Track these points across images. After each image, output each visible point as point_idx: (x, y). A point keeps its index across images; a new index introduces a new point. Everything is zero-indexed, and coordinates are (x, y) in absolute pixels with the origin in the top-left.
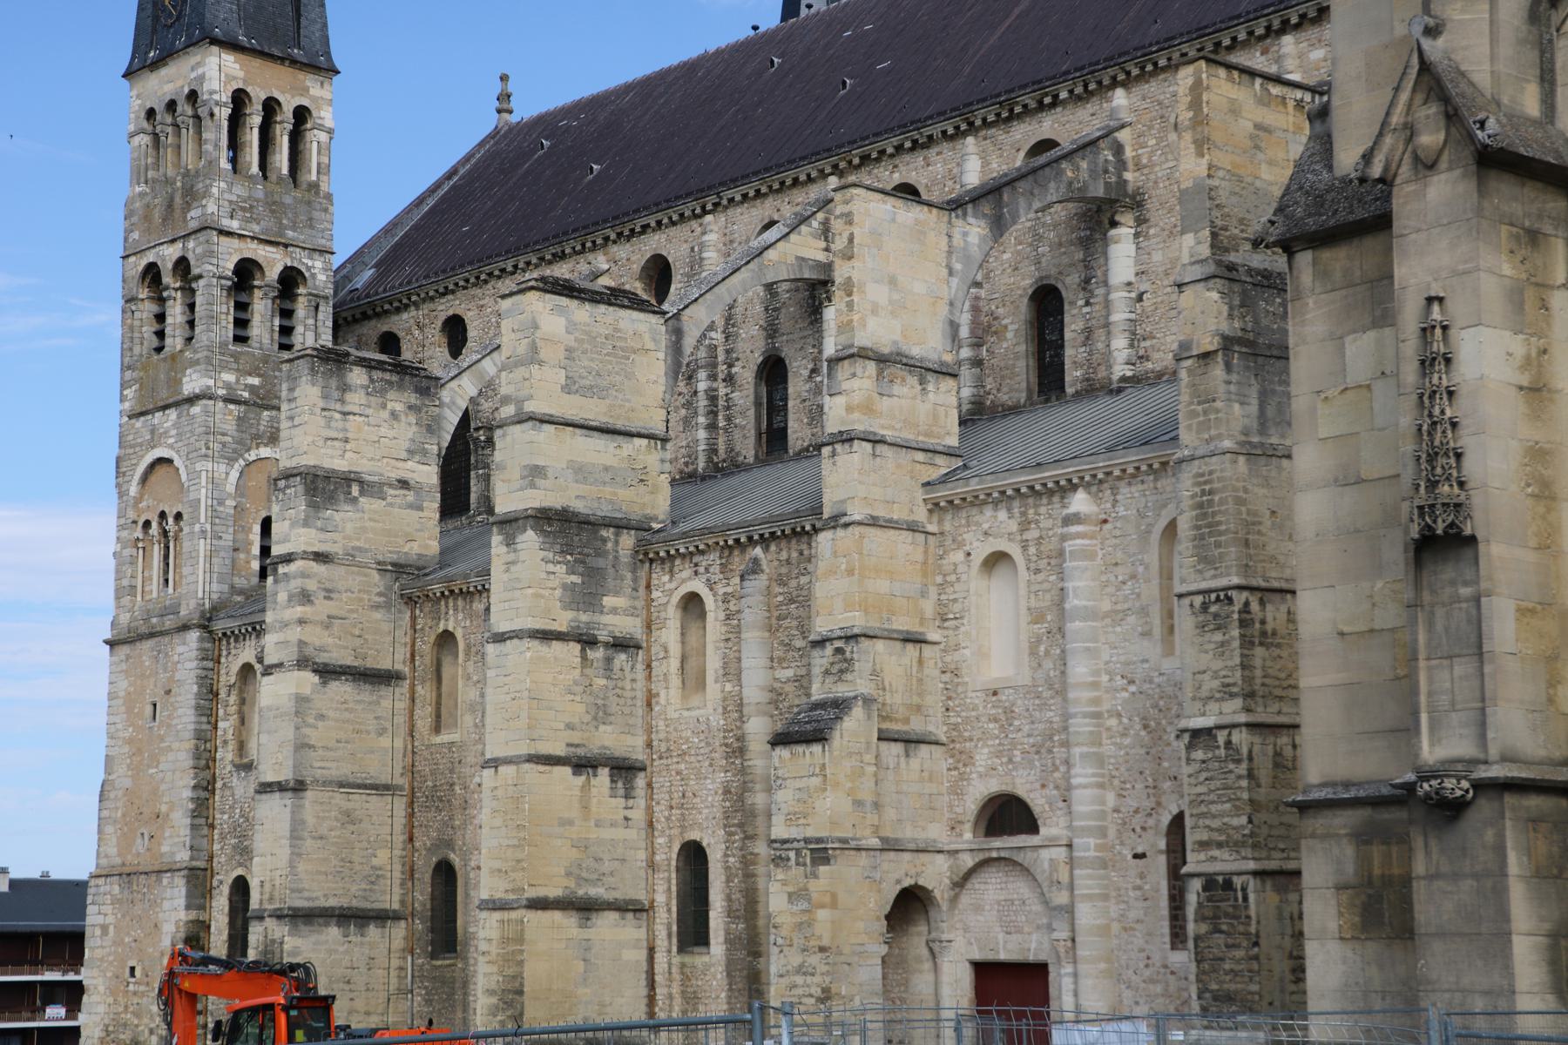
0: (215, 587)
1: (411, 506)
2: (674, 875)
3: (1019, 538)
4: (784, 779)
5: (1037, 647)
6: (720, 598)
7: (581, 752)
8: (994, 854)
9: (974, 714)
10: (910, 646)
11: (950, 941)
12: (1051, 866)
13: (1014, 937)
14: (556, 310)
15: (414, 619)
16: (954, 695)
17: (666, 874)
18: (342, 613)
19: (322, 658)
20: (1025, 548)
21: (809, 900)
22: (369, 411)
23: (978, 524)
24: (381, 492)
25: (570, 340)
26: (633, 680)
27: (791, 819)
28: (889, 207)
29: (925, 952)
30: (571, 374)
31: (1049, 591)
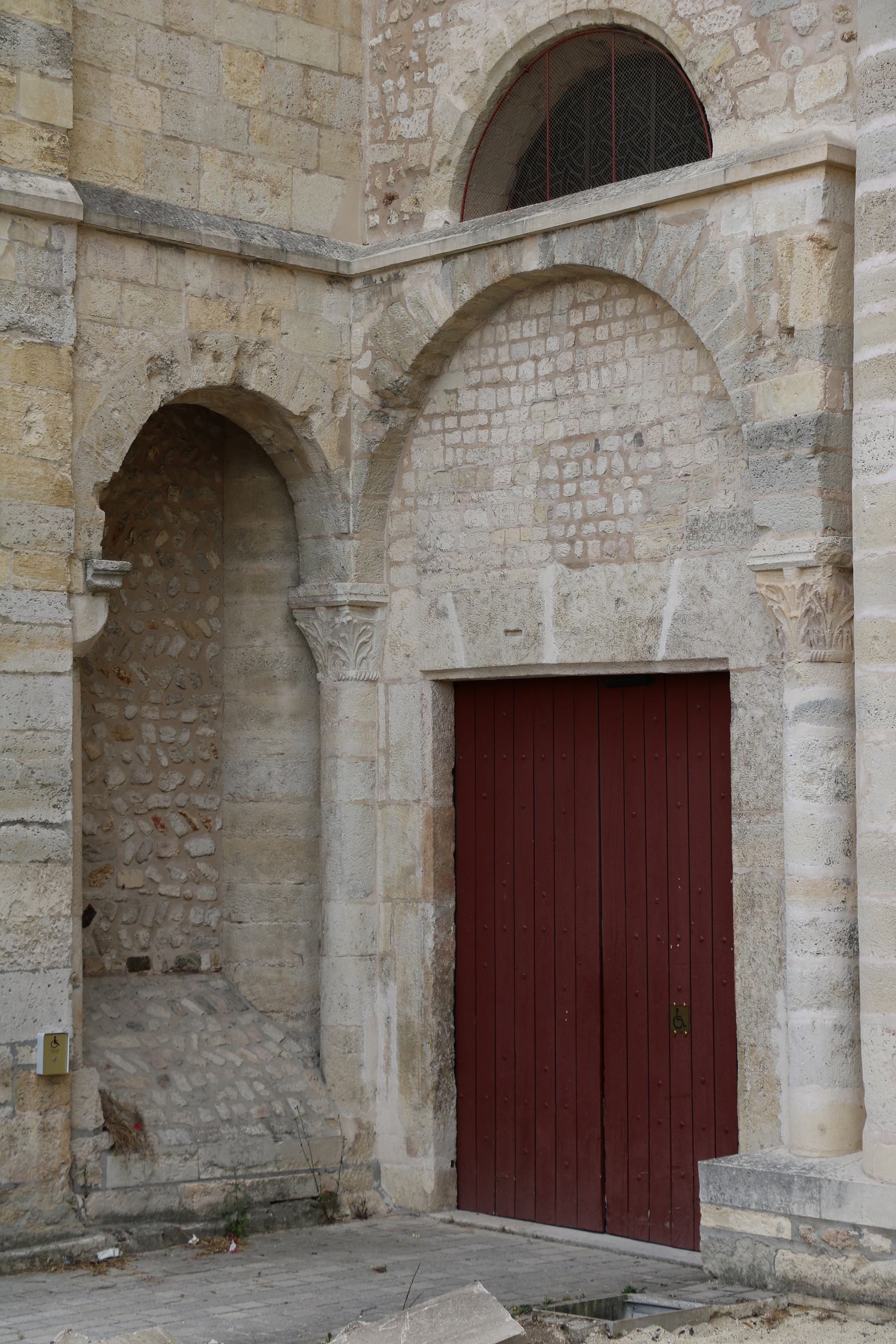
11: (368, 608)
12: (754, 265)
13: (598, 575)
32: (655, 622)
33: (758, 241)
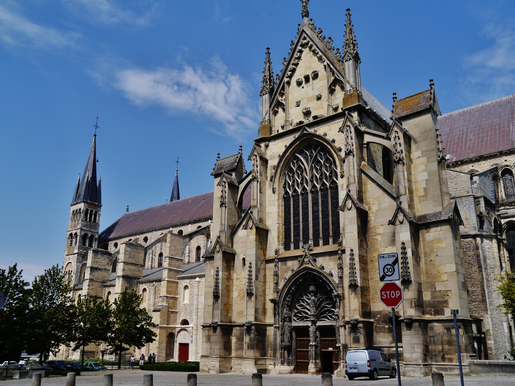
0: (76, 282)
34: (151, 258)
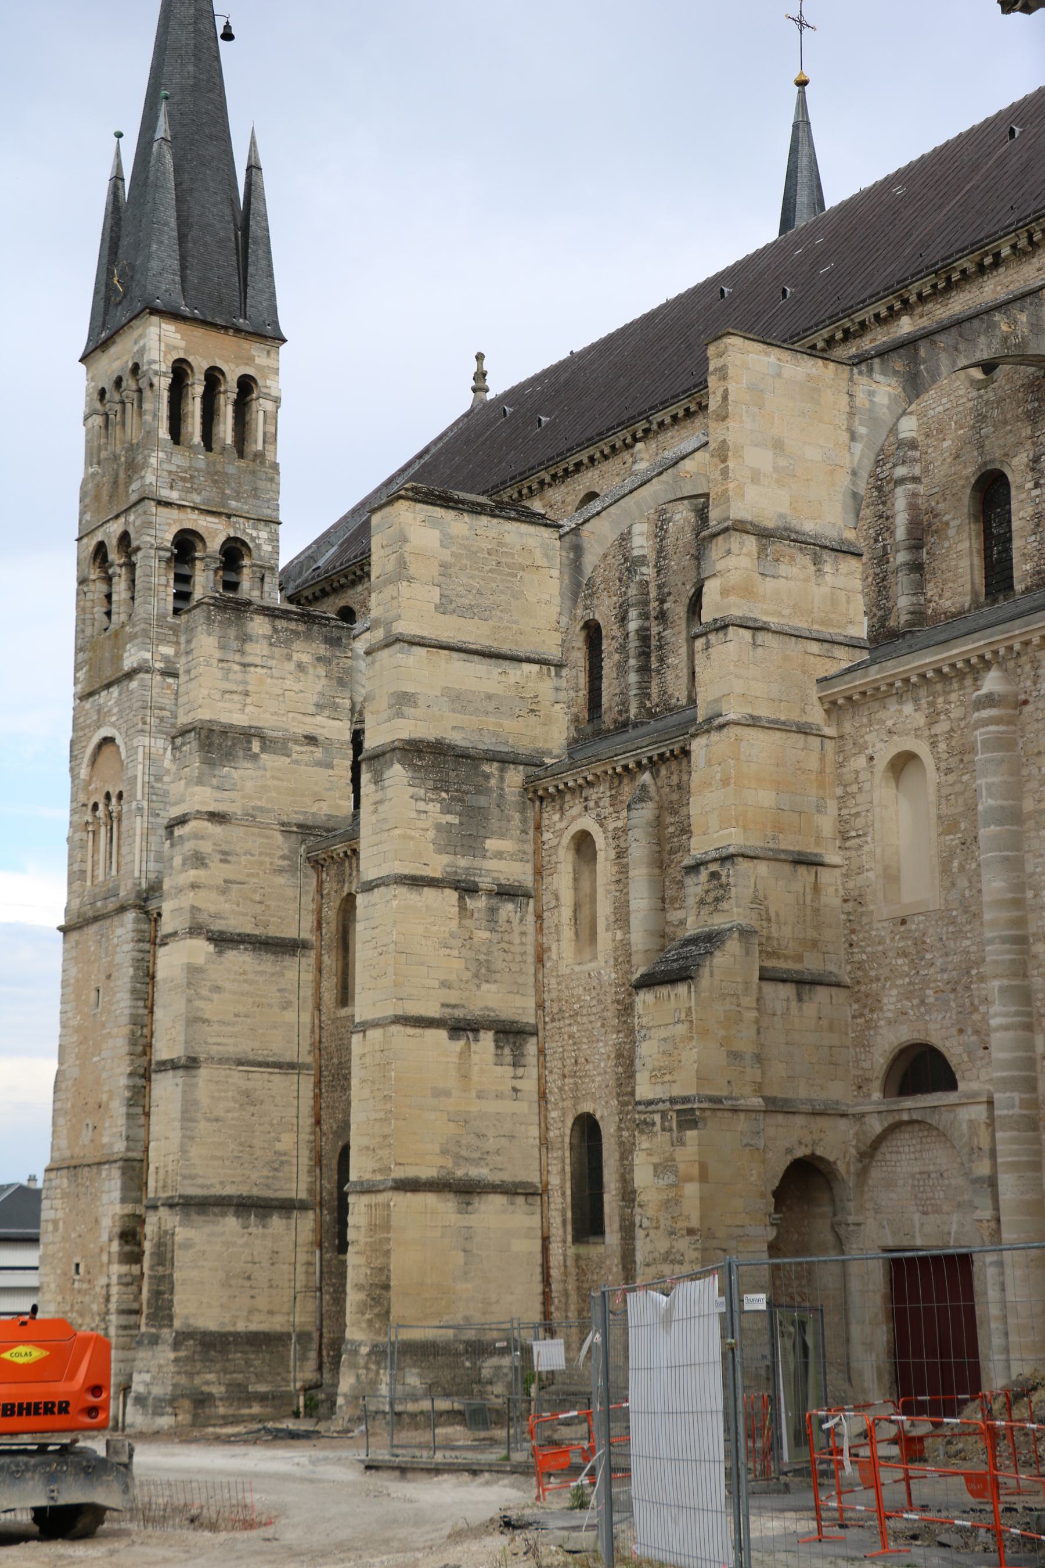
1: (319, 764)
2: (567, 1154)
3: (927, 733)
4: (649, 1029)
5: (951, 862)
6: (610, 835)
7: (459, 1013)
8: (905, 1117)
9: (880, 948)
10: (802, 870)
11: (859, 1224)
12: (970, 1128)
13: (932, 1218)
14: (434, 522)
15: (320, 884)
16: (856, 927)
17: (560, 1153)
18: (241, 878)
19: (217, 926)
20: (934, 745)
21: (676, 1173)
22: (272, 663)
23: (881, 722)
24: (286, 748)
25: (446, 555)
26: (523, 934)
27: (657, 1075)
28: (772, 359)
29: (829, 1237)
30: (446, 593)
31: (963, 793)
32: (949, 1233)
33: (970, 1121)
34: (633, 643)
